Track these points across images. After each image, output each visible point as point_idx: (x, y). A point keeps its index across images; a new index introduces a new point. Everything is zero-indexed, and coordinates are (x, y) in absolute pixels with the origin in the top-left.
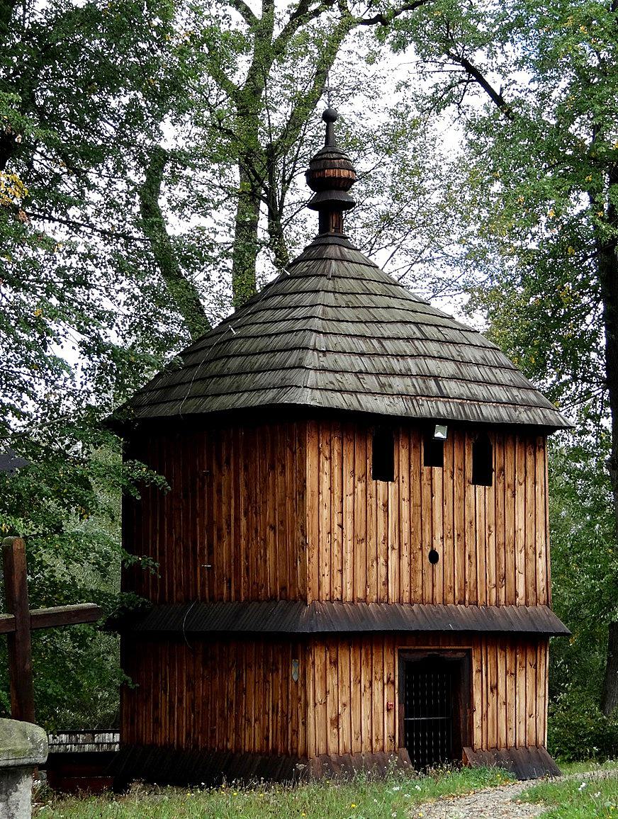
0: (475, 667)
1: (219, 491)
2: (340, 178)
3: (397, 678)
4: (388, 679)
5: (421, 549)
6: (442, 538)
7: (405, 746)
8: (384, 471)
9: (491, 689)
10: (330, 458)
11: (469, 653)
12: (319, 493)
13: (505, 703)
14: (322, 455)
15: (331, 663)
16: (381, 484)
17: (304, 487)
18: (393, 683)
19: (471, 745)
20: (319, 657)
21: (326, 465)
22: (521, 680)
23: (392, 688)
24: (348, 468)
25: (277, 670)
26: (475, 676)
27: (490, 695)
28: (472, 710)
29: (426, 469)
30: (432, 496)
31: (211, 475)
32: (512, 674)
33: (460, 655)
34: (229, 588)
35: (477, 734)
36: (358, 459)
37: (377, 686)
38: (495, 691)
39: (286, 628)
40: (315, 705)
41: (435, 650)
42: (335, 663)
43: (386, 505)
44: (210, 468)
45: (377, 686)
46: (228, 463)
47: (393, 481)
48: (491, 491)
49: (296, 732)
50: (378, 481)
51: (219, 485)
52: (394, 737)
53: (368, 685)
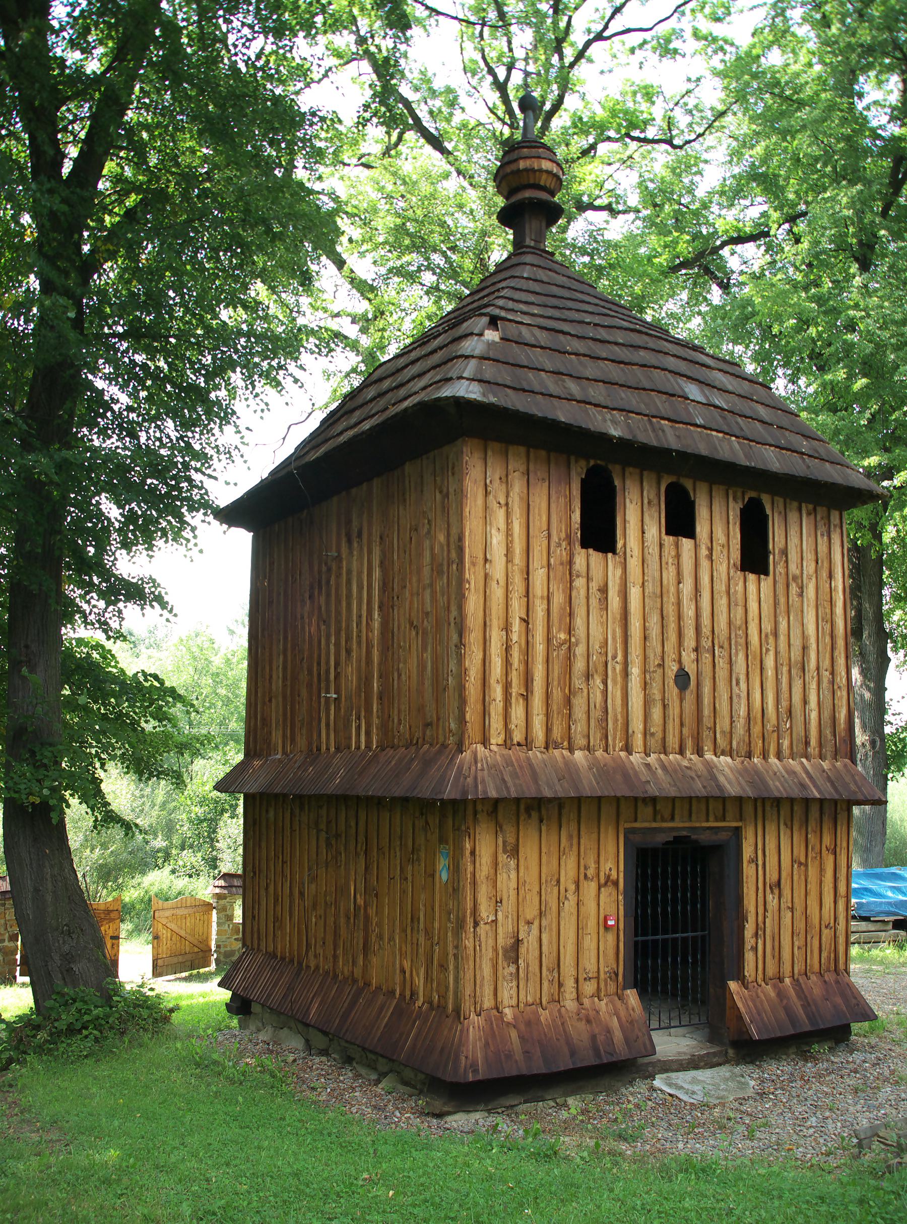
0: (747, 851)
1: (349, 582)
2: (541, 171)
3: (621, 875)
4: (608, 878)
5: (662, 665)
6: (696, 650)
7: (635, 986)
8: (599, 533)
9: (771, 888)
10: (507, 504)
11: (737, 831)
12: (486, 560)
13: (792, 909)
14: (491, 497)
15: (505, 851)
16: (595, 557)
17: (461, 550)
18: (616, 884)
19: (740, 977)
20: (484, 846)
21: (501, 514)
22: (813, 871)
23: (614, 893)
24: (539, 521)
25: (418, 860)
26: (748, 871)
27: (770, 897)
28: (741, 918)
29: (669, 540)
30: (679, 583)
31: (339, 559)
32: (800, 864)
33: (723, 836)
34: (358, 728)
35: (749, 956)
36: (556, 507)
37: (590, 889)
38: (776, 891)
39: (425, 791)
40: (476, 924)
41: (684, 828)
42: (514, 852)
43: (604, 590)
44: (339, 551)
45: (590, 889)
46: (360, 535)
47: (614, 552)
48: (766, 583)
49: (443, 967)
50: (591, 551)
51: (349, 572)
52: (617, 975)
53: (572, 887)
